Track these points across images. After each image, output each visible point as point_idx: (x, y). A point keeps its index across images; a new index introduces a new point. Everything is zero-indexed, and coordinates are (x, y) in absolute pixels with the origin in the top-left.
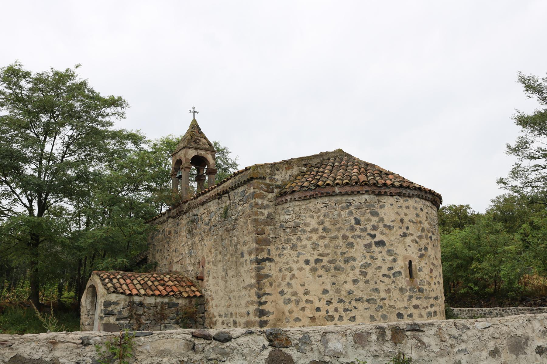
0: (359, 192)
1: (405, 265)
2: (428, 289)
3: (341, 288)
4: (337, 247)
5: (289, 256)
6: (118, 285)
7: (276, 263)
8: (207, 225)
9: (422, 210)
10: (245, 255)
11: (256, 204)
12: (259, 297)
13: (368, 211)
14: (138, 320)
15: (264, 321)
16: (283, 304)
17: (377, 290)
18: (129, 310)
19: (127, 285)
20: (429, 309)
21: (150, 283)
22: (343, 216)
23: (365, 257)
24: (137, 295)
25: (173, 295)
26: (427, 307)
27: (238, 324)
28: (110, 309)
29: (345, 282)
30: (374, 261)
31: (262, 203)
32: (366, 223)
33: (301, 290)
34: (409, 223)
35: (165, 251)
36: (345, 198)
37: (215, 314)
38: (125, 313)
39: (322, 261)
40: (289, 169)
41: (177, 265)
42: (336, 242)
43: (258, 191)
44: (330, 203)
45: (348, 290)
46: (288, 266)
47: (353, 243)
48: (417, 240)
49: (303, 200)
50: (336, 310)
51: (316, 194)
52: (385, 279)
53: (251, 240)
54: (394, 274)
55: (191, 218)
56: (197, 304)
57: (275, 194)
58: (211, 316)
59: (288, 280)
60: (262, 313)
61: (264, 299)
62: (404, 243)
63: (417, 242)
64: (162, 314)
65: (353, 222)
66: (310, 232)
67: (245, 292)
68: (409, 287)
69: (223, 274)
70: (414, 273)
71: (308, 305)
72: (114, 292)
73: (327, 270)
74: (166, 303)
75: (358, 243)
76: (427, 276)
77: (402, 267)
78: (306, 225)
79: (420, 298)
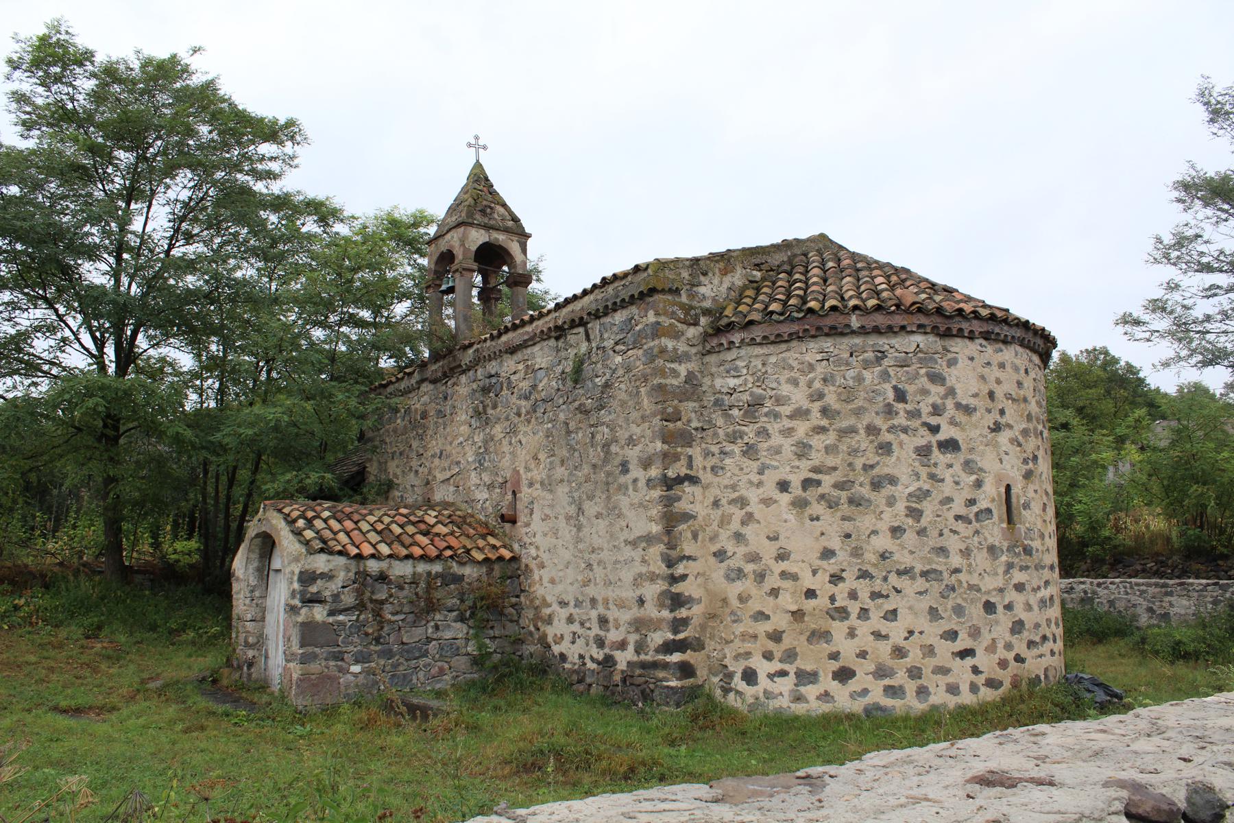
0: (903, 328)
1: (999, 495)
2: (1040, 548)
3: (864, 546)
4: (854, 452)
5: (737, 472)
6: (327, 534)
7: (706, 487)
8: (527, 398)
9: (1026, 372)
10: (631, 467)
11: (663, 351)
12: (670, 564)
13: (923, 371)
14: (378, 614)
15: (682, 619)
16: (723, 580)
17: (942, 551)
18: (357, 590)
19: (348, 534)
21: (397, 530)
22: (867, 382)
23: (917, 476)
24: (373, 556)
25: (451, 557)
26: (1039, 588)
27: (611, 625)
28: (314, 589)
29: (875, 532)
30: (936, 484)
31: (675, 350)
32: (919, 398)
33: (768, 551)
35: (413, 455)
36: (872, 340)
37: (549, 599)
38: (349, 599)
39: (819, 483)
40: (726, 274)
41: (444, 486)
42: (853, 441)
43: (666, 321)
44: (836, 352)
45: (881, 551)
46: (737, 494)
47: (889, 444)
48: (1020, 438)
49: (773, 343)
50: (853, 595)
51: (806, 330)
52: (960, 526)
53: (649, 433)
54: (977, 514)
55: (481, 383)
56: (503, 578)
57: (701, 329)
58: (537, 603)
59: (735, 525)
60: (677, 601)
61: (680, 569)
62: (996, 445)
63: (1020, 445)
64: (429, 601)
65: (891, 395)
66: (791, 417)
67: (633, 553)
68: (1006, 544)
69: (572, 510)
70: (1015, 512)
71: (787, 584)
72: (322, 550)
73: (832, 505)
74: (438, 575)
75: (901, 444)
77: (993, 500)
78: (779, 401)
79: (1027, 568)
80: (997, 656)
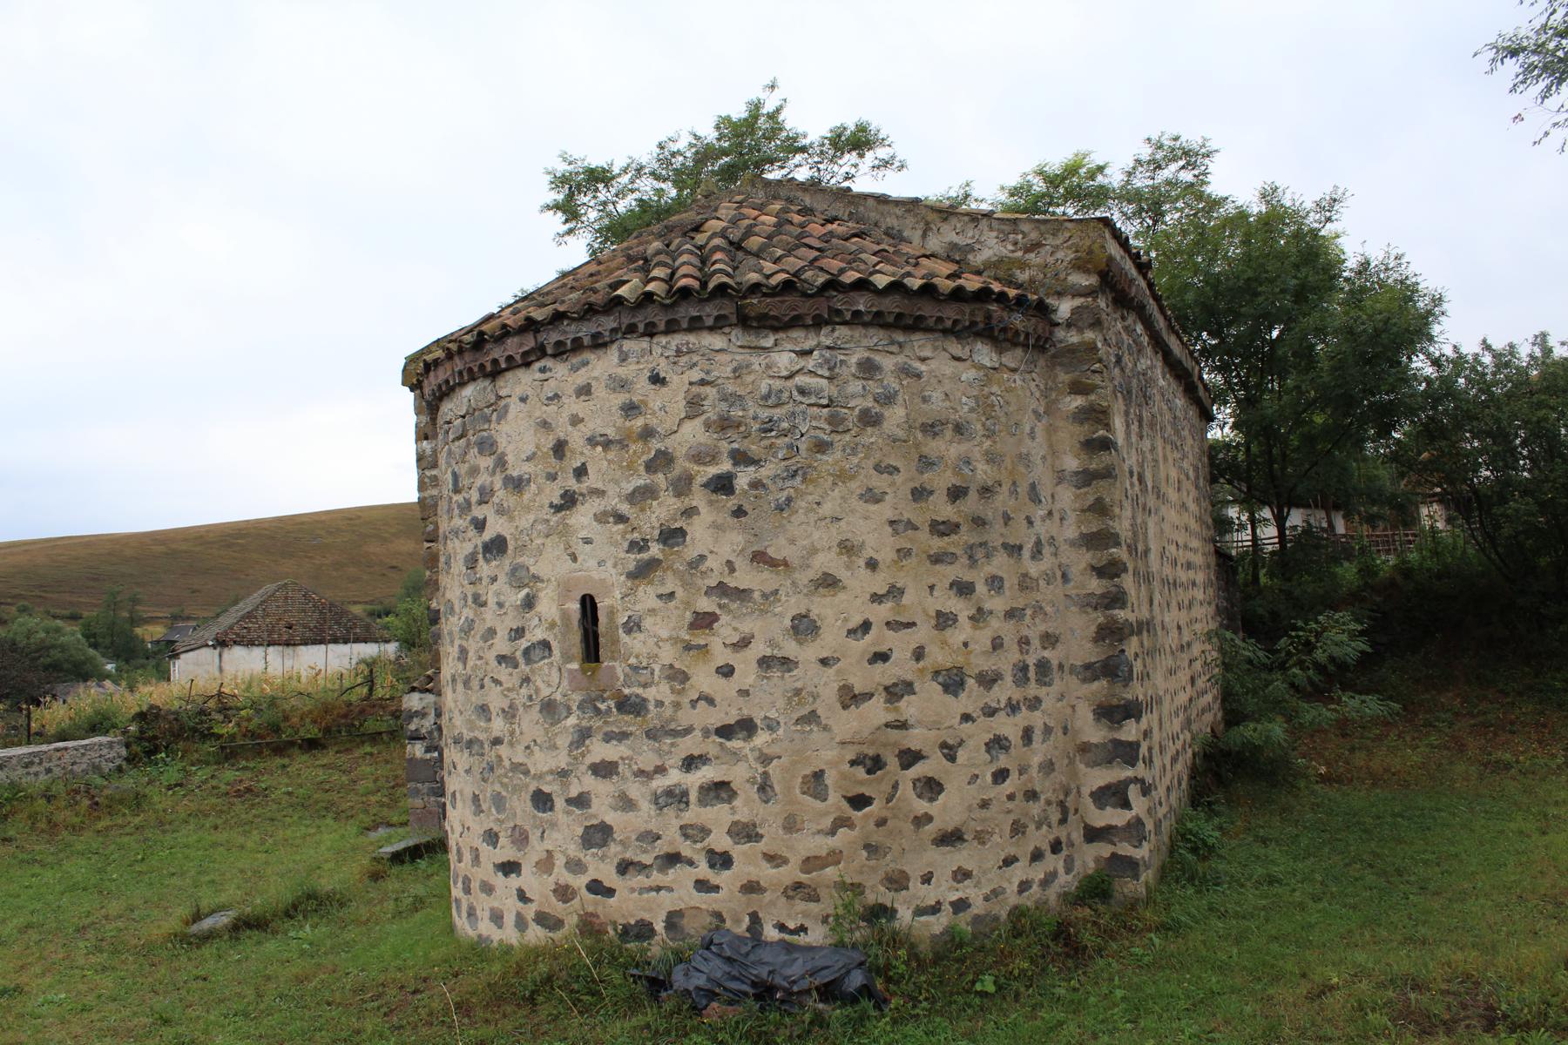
1: (565, 615)
2: (668, 698)
20: (675, 777)
26: (661, 770)
34: (587, 450)
48: (624, 508)
52: (503, 673)
54: (527, 652)
62: (564, 531)
63: (621, 518)
68: (577, 697)
76: (667, 647)
77: (552, 625)
79: (623, 736)
80: (552, 879)
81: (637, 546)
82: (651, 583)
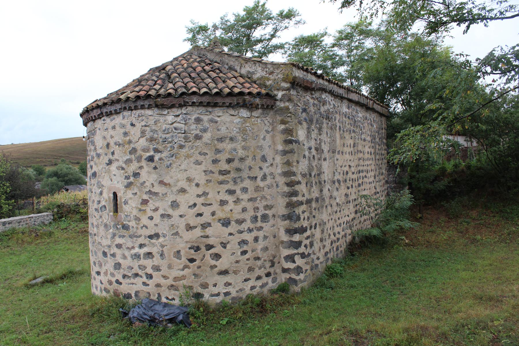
1: (109, 197)
2: (135, 226)
20: (137, 250)
26: (133, 248)
34: (114, 146)
48: (124, 165)
54: (101, 208)
62: (109, 171)
63: (123, 169)
68: (112, 223)
76: (134, 210)
79: (124, 236)
80: (107, 278)
81: (127, 178)
82: (130, 189)
